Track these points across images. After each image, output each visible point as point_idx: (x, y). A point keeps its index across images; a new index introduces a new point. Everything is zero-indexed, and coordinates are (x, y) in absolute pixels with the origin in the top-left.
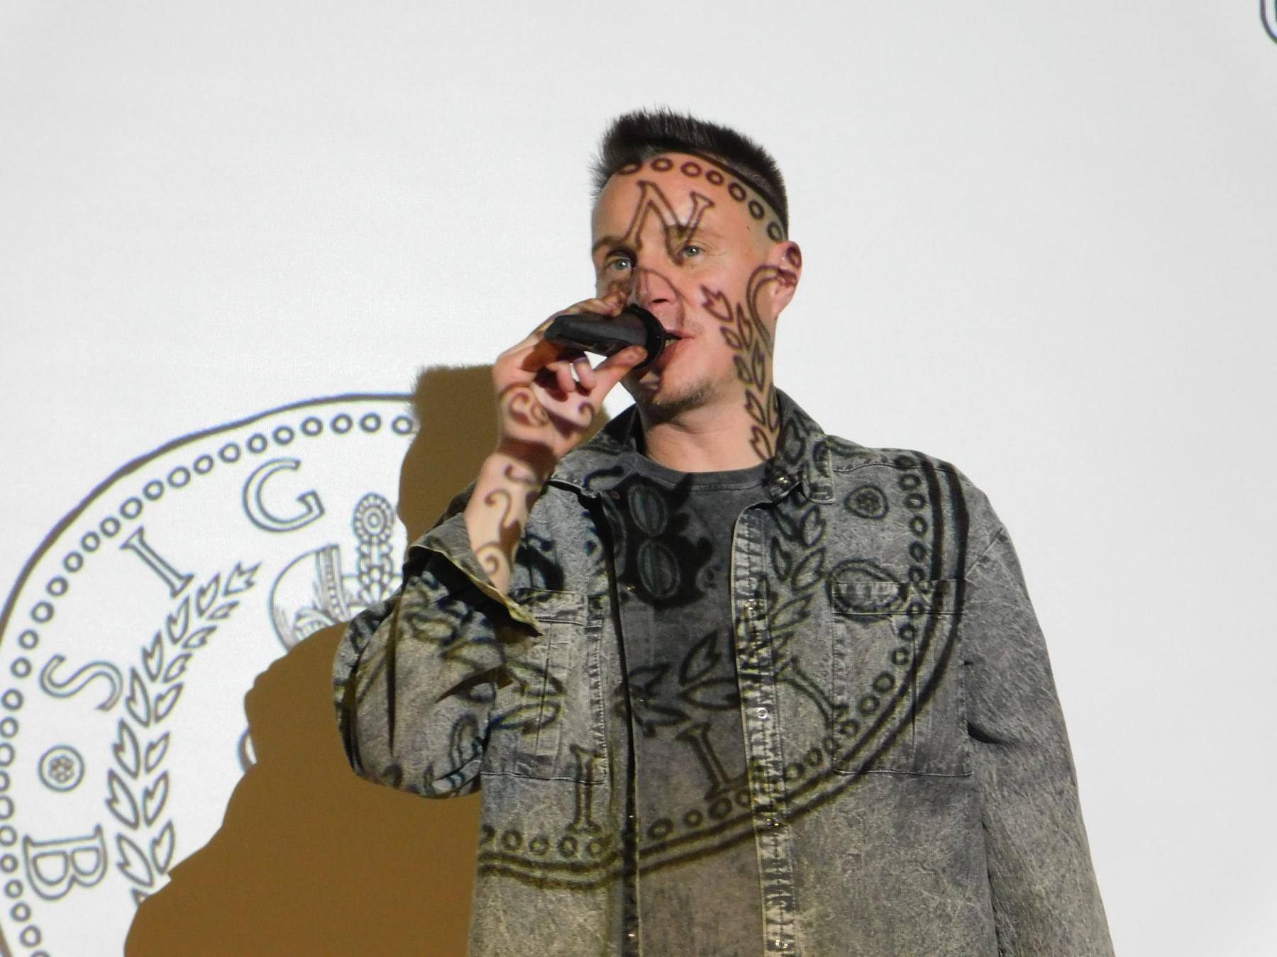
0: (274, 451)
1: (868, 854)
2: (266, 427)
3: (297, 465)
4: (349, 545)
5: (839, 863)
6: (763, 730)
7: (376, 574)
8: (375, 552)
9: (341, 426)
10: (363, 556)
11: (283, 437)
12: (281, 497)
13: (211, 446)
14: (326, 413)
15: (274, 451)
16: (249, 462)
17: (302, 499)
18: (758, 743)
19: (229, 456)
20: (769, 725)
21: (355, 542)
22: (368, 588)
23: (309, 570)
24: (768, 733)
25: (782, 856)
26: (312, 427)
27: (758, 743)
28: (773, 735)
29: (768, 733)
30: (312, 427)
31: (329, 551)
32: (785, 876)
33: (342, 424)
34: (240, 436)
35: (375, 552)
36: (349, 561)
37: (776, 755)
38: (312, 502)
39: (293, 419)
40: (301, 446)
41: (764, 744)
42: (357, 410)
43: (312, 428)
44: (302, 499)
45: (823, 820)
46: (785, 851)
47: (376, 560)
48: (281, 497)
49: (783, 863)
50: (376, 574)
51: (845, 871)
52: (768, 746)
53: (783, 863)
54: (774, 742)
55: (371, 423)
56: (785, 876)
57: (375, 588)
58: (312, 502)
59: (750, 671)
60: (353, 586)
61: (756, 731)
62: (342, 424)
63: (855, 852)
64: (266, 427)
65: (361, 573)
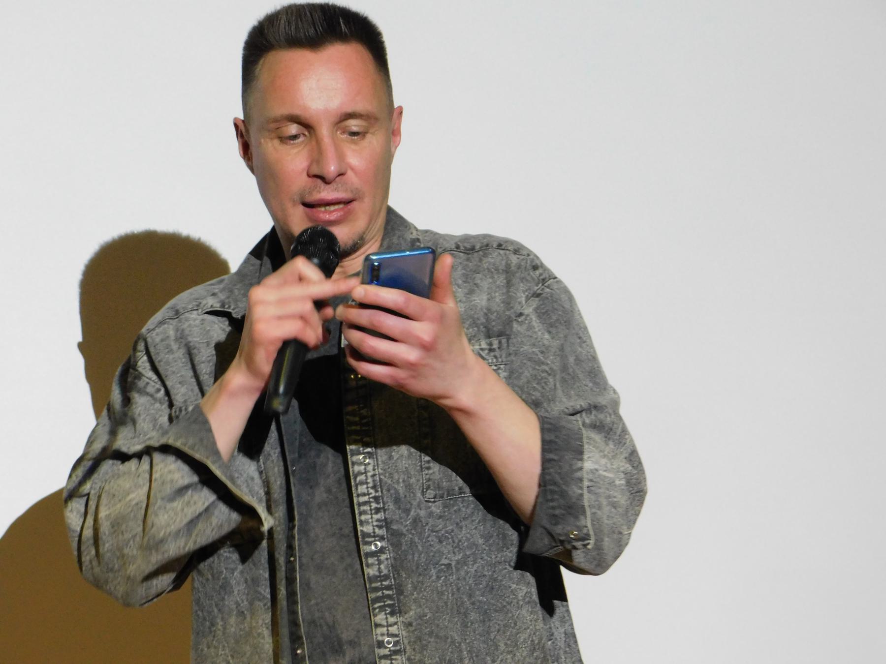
1: (458, 562)
5: (433, 572)
6: (365, 473)
18: (362, 483)
20: (370, 468)
24: (369, 474)
25: (385, 572)
27: (362, 483)
28: (374, 476)
29: (369, 474)
32: (388, 588)
37: (376, 491)
41: (367, 483)
45: (416, 540)
46: (387, 567)
49: (387, 577)
51: (438, 578)
52: (370, 485)
53: (387, 577)
54: (374, 481)
56: (388, 588)
59: (354, 428)
61: (360, 473)
63: (446, 562)
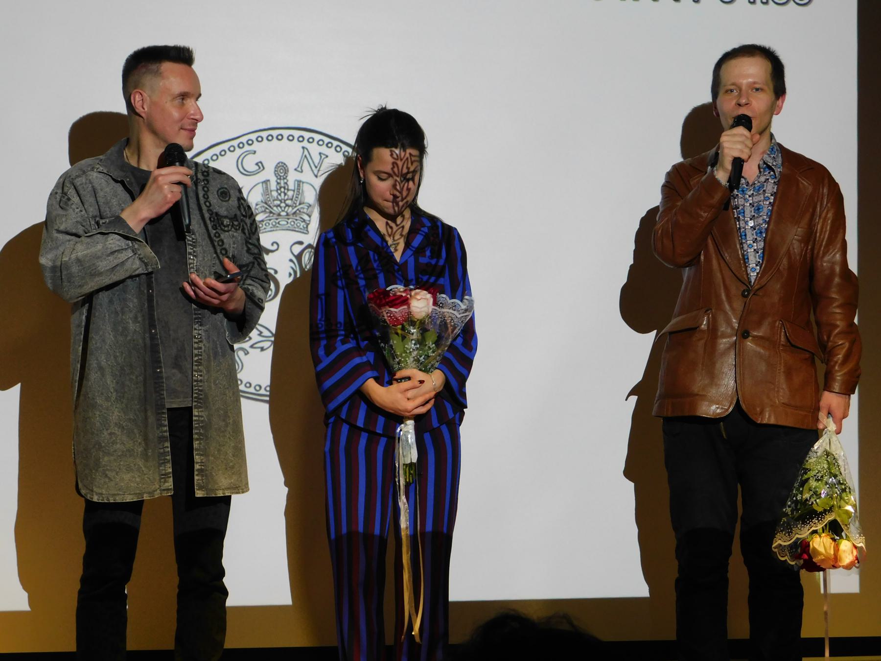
0: (247, 148)
2: (244, 139)
3: (255, 152)
4: (273, 180)
7: (283, 190)
8: (282, 182)
9: (269, 138)
10: (278, 183)
11: (250, 143)
12: (250, 164)
13: (225, 146)
14: (264, 134)
15: (247, 148)
16: (238, 152)
17: (257, 164)
19: (232, 150)
21: (275, 179)
22: (280, 194)
23: (259, 189)
26: (260, 139)
30: (260, 139)
31: (266, 182)
33: (270, 138)
34: (235, 143)
35: (282, 182)
36: (273, 185)
38: (260, 165)
39: (253, 137)
40: (256, 146)
42: (275, 133)
43: (260, 140)
44: (257, 164)
47: (282, 185)
48: (250, 164)
50: (283, 190)
55: (280, 137)
57: (283, 195)
58: (260, 165)
60: (275, 194)
62: (270, 138)
64: (244, 139)
65: (277, 190)
